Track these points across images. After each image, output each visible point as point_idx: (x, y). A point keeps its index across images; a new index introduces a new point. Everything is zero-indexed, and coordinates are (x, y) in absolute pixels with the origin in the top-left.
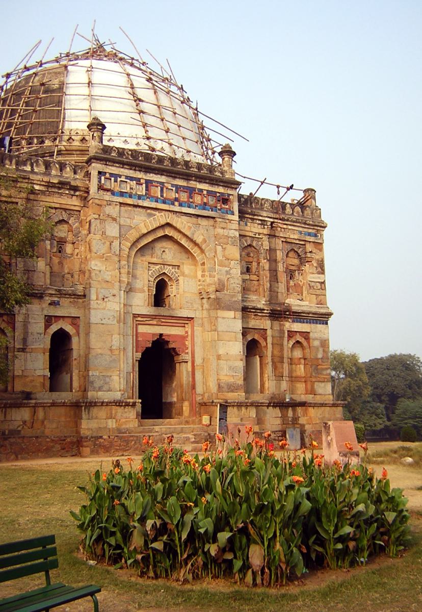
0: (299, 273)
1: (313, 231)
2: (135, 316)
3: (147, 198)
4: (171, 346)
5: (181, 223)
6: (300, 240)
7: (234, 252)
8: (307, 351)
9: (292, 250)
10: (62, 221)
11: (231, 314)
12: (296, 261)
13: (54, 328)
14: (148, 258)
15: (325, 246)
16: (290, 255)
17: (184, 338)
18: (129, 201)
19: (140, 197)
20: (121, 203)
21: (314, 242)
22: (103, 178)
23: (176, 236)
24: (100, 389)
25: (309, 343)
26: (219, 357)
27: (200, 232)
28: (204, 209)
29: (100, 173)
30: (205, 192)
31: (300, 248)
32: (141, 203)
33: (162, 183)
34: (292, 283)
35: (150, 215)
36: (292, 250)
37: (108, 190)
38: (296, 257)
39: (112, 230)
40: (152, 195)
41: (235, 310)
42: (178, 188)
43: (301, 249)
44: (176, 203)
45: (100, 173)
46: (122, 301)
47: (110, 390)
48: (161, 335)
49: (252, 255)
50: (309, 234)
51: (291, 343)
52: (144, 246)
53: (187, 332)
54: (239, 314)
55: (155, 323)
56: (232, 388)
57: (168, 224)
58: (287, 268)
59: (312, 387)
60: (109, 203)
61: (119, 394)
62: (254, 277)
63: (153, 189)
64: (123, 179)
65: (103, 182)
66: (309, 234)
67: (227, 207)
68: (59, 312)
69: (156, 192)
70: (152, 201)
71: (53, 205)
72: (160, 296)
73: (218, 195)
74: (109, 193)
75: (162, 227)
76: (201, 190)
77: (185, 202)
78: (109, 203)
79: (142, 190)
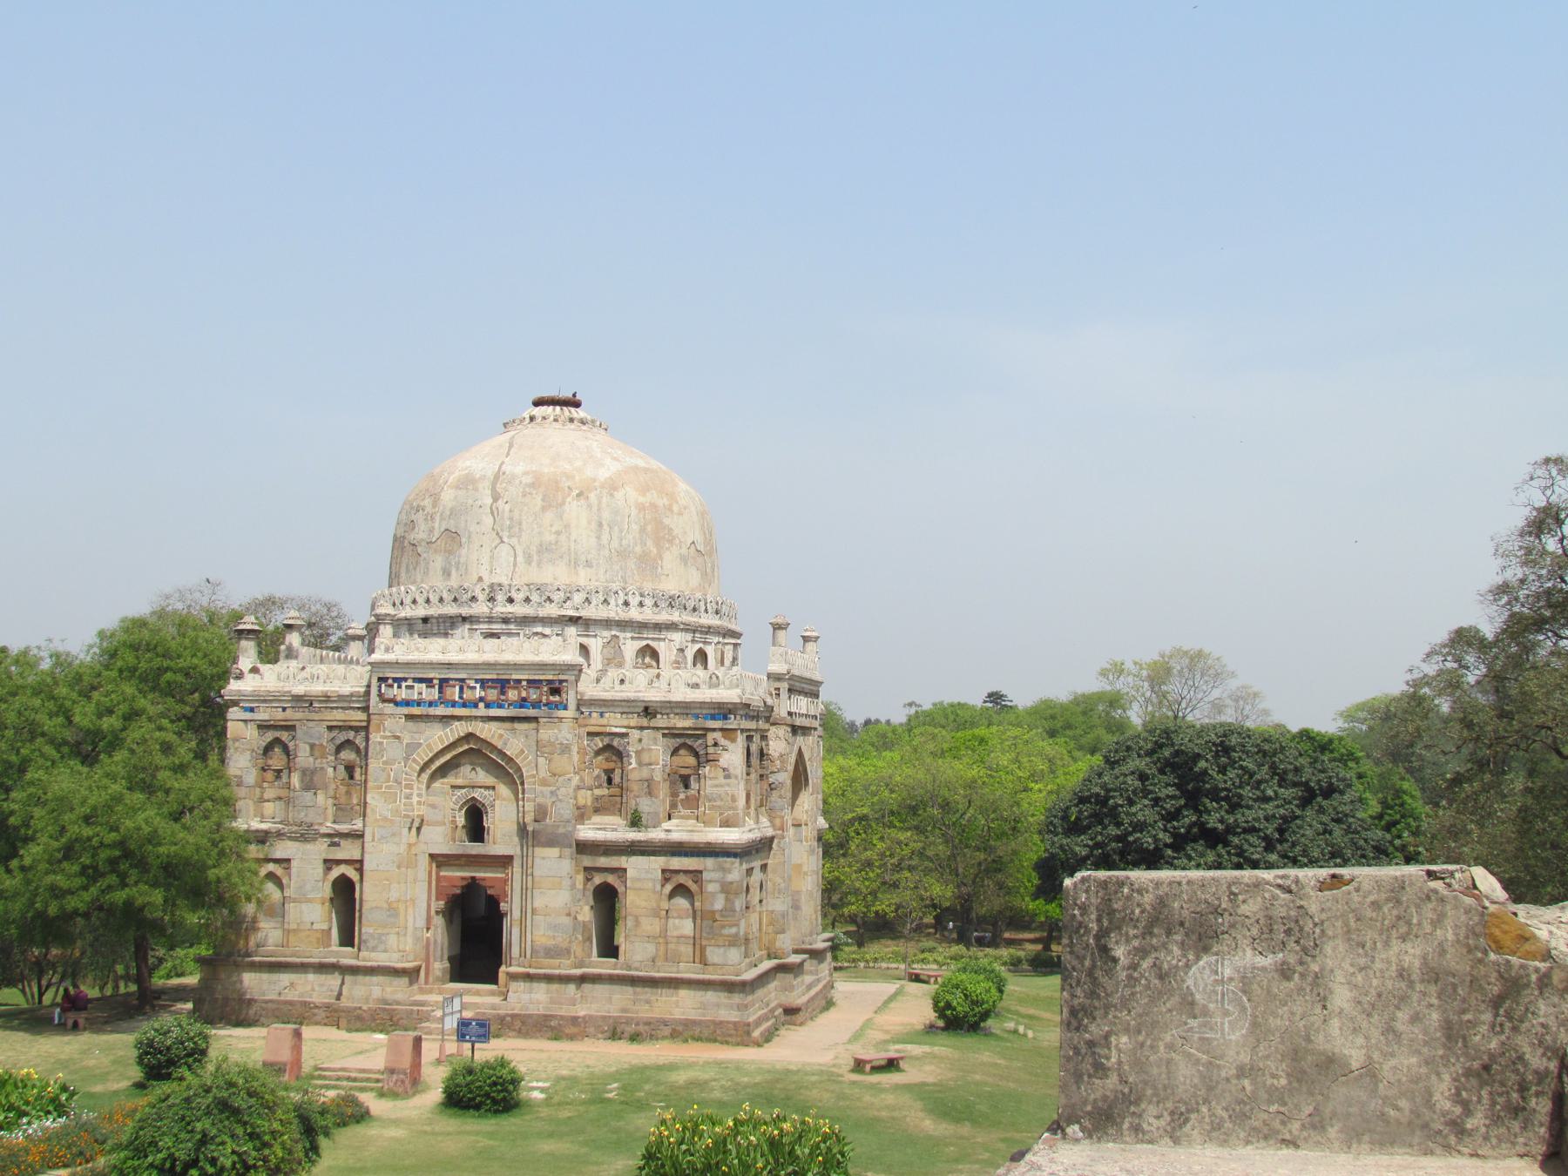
2: (432, 856)
9: (684, 745)
10: (348, 741)
11: (555, 852)
12: (692, 761)
13: (336, 872)
14: (451, 780)
16: (682, 752)
17: (506, 881)
18: (416, 711)
19: (431, 704)
21: (721, 730)
24: (374, 949)
25: (701, 888)
26: (534, 911)
29: (380, 679)
33: (463, 680)
34: (682, 796)
39: (395, 751)
42: (484, 683)
44: (481, 705)
45: (380, 679)
46: (404, 840)
47: (385, 951)
50: (713, 717)
51: (669, 888)
52: (442, 768)
56: (552, 952)
57: (470, 737)
61: (396, 956)
63: (448, 691)
64: (410, 683)
68: (340, 856)
72: (475, 823)
79: (434, 694)
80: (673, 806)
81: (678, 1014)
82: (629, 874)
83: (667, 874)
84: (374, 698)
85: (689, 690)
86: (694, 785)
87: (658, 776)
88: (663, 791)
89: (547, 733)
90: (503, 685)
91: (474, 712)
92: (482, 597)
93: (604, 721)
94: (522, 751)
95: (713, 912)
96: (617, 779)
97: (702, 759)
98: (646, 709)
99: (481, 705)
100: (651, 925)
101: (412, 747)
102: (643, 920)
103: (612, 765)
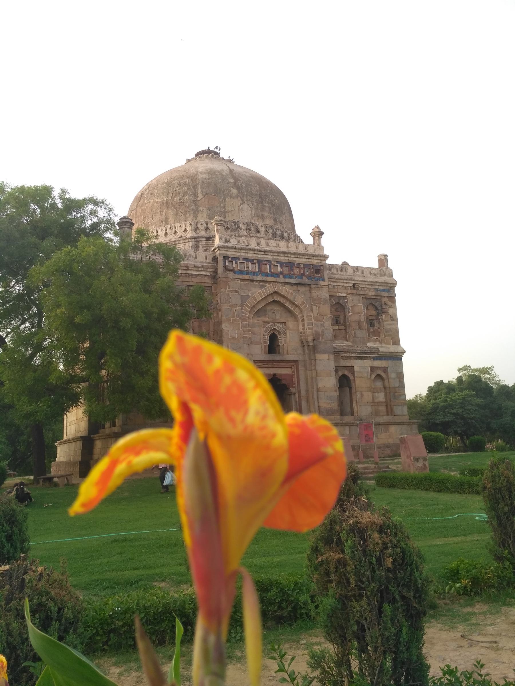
0: (377, 322)
1: (388, 288)
3: (260, 273)
4: (283, 382)
5: (285, 290)
6: (376, 296)
7: (326, 309)
8: (386, 381)
11: (325, 357)
12: (374, 312)
14: (263, 319)
15: (397, 298)
16: (369, 308)
18: (246, 277)
19: (254, 273)
20: (240, 279)
22: (227, 261)
23: (282, 300)
27: (299, 298)
28: (302, 278)
29: (224, 257)
30: (302, 266)
31: (376, 302)
32: (255, 278)
33: (270, 262)
34: (372, 330)
35: (262, 287)
36: (371, 303)
37: (230, 270)
38: (374, 309)
39: (236, 299)
40: (263, 271)
41: (330, 353)
42: (282, 264)
43: (378, 303)
44: (281, 276)
48: (275, 375)
49: (339, 310)
50: (384, 290)
51: (373, 376)
53: (293, 372)
54: (332, 357)
55: (270, 366)
57: (276, 292)
58: (367, 318)
59: (392, 409)
60: (233, 279)
62: (342, 327)
63: (263, 267)
65: (227, 264)
66: (384, 290)
67: (319, 275)
69: (267, 268)
70: (262, 276)
71: (191, 284)
73: (312, 266)
74: (232, 273)
75: (271, 294)
76: (299, 264)
77: (288, 275)
78: (233, 279)
79: (256, 268)
80: (369, 335)
81: (390, 441)
82: (356, 369)
83: (372, 369)
84: (221, 270)
85: (372, 276)
86: (376, 324)
87: (363, 319)
88: (365, 326)
89: (315, 293)
90: (291, 265)
91: (278, 280)
92: (244, 228)
93: (336, 290)
94: (303, 303)
95: (395, 388)
96: (342, 321)
97: (380, 312)
98: (354, 284)
99: (281, 276)
100: (368, 396)
101: (244, 299)
102: (364, 393)
103: (338, 314)
